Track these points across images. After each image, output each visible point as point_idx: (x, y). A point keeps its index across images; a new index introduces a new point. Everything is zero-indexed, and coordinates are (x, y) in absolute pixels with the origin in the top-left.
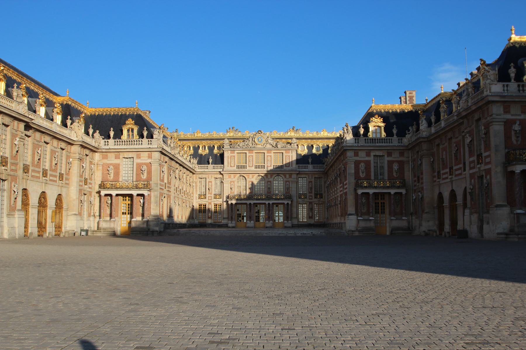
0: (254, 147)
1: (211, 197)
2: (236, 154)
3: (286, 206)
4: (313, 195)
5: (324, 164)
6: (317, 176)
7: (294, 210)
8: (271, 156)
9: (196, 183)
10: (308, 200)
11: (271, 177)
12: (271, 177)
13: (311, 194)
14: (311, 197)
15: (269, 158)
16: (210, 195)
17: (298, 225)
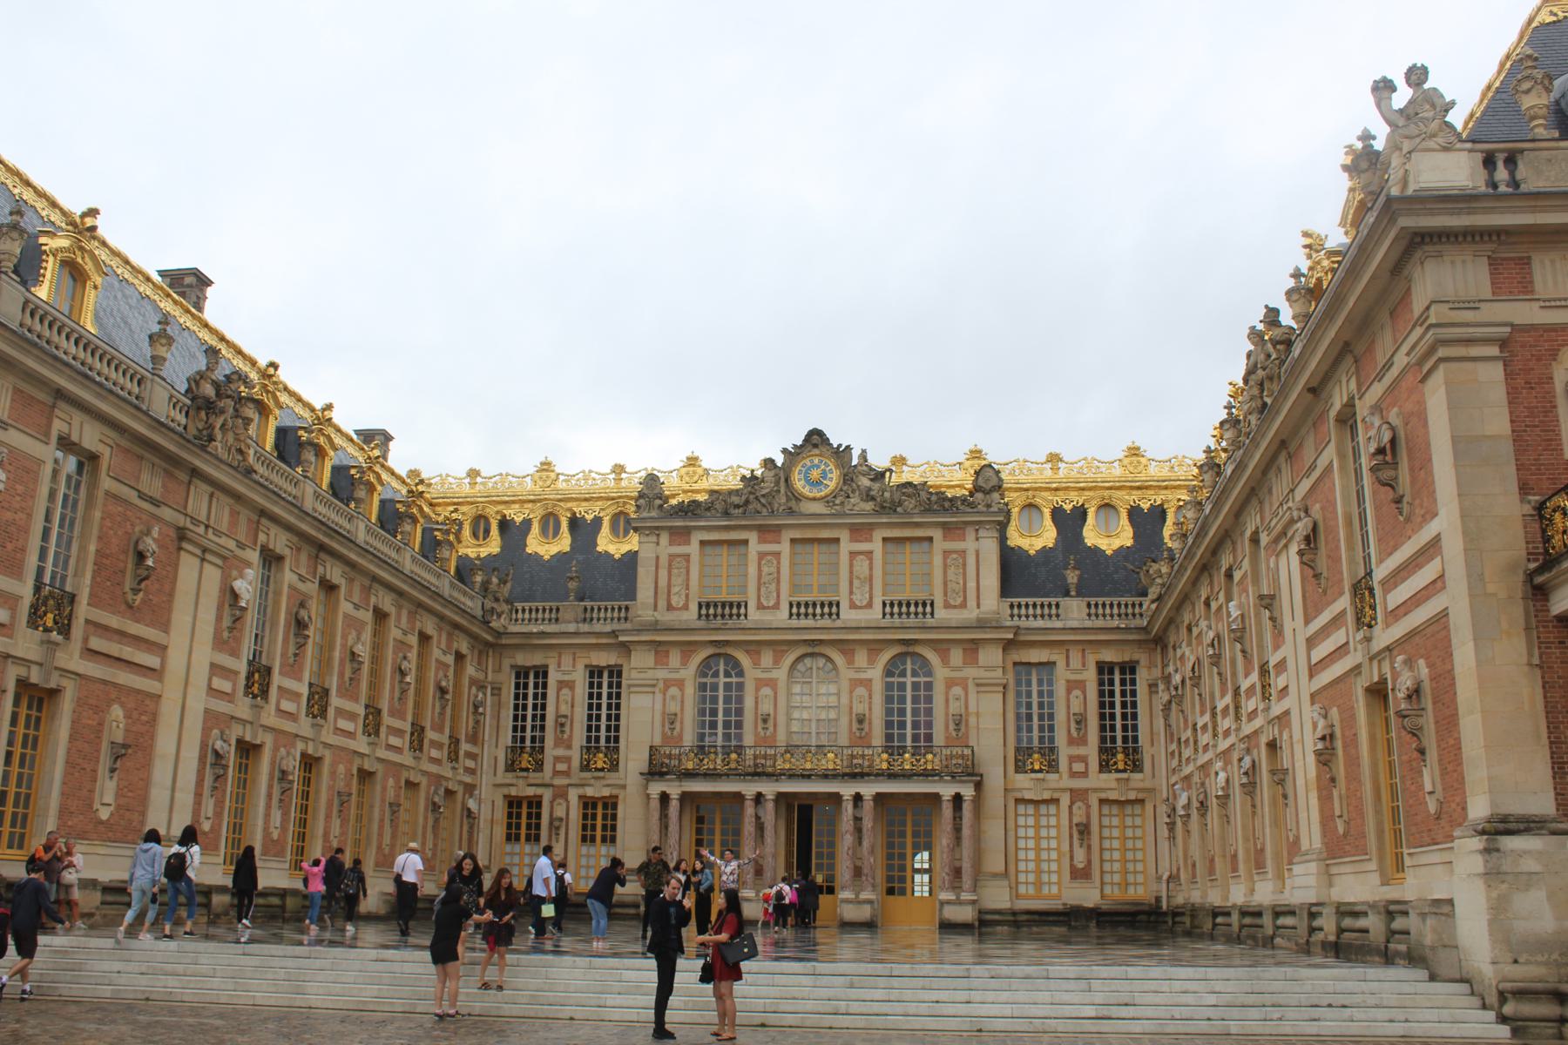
0: (791, 512)
1: (568, 760)
2: (693, 548)
3: (947, 810)
4: (1091, 750)
5: (1145, 594)
6: (1109, 656)
7: (994, 831)
8: (869, 554)
9: (497, 691)
10: (1067, 782)
11: (871, 661)
12: (871, 661)
13: (1081, 751)
14: (1079, 767)
15: (861, 566)
16: (560, 752)
17: (1014, 913)
